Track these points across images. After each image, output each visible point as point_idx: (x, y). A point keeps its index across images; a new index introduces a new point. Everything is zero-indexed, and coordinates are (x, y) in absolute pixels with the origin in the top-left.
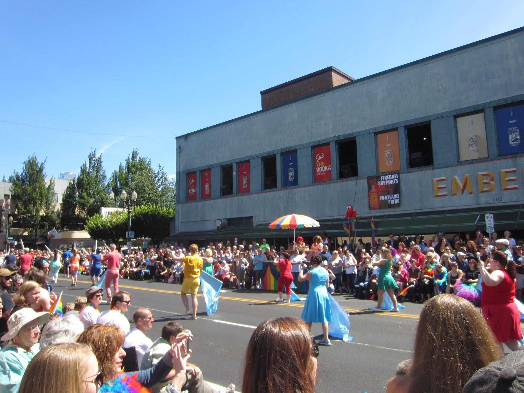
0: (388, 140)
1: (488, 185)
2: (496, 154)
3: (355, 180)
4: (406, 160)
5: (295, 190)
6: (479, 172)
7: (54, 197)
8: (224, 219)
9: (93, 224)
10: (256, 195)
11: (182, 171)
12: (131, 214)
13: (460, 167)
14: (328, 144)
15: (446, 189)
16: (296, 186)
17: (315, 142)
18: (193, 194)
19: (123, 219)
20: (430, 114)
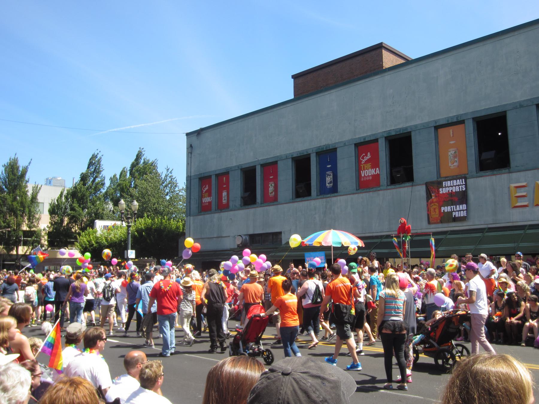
0: (452, 135)
3: (411, 186)
4: (474, 161)
5: (334, 199)
7: (39, 207)
8: (245, 235)
9: (85, 240)
10: (285, 205)
11: (194, 175)
12: (131, 229)
14: (376, 141)
15: (526, 198)
16: (336, 194)
17: (360, 138)
18: (207, 204)
19: (122, 235)
20: (506, 103)
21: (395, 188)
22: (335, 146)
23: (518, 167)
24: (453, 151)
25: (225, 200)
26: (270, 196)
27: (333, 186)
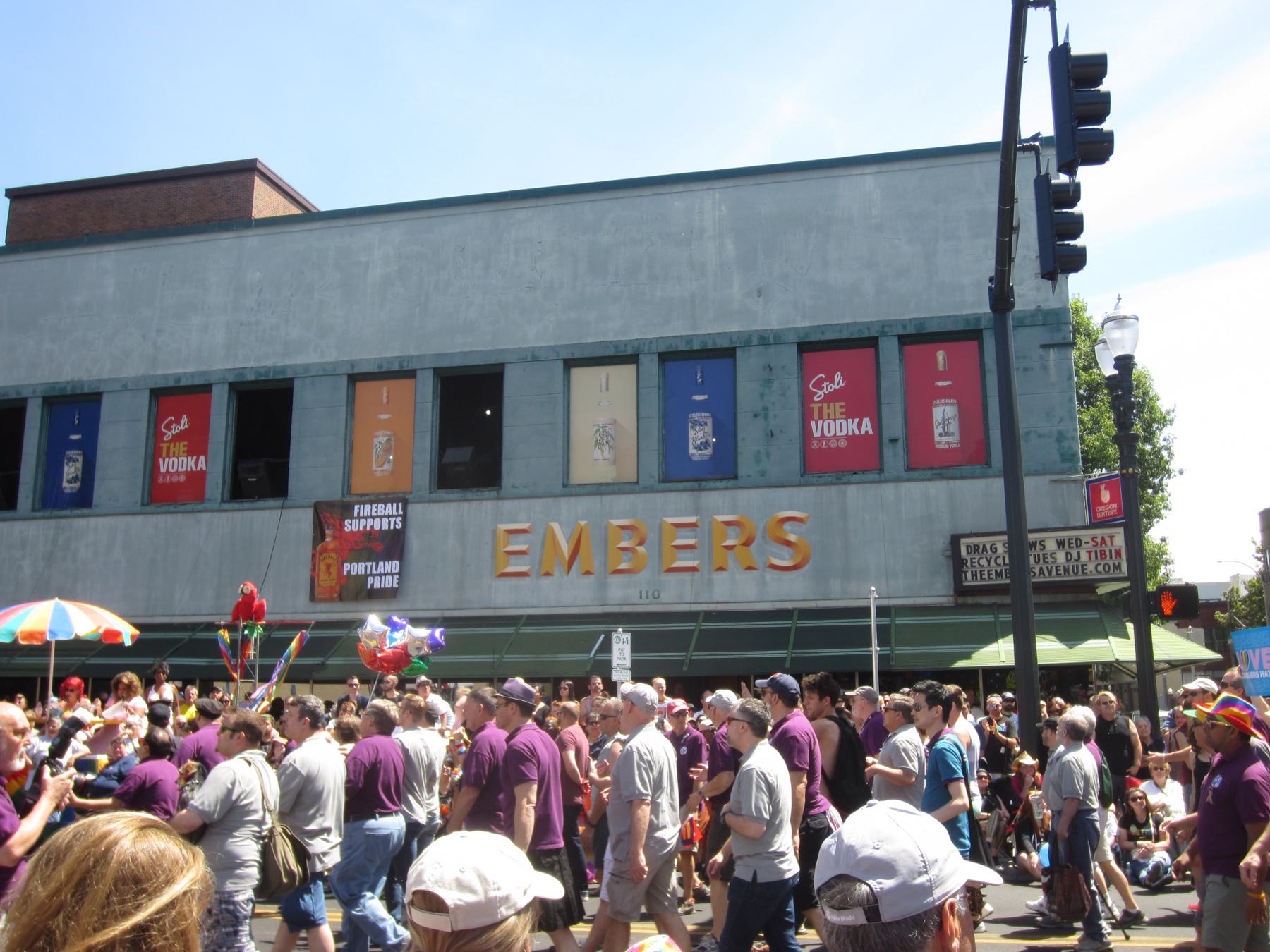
0: (385, 400)
1: (630, 554)
2: (656, 474)
3: (492, 499)
4: (428, 465)
6: (611, 518)
13: (566, 499)
15: (526, 557)
16: (86, 511)
17: (165, 377)
21: (239, 510)
22: (99, 388)
23: (517, 487)
24: (385, 436)
25: (947, 434)
26: (378, 474)
27: (712, 457)
